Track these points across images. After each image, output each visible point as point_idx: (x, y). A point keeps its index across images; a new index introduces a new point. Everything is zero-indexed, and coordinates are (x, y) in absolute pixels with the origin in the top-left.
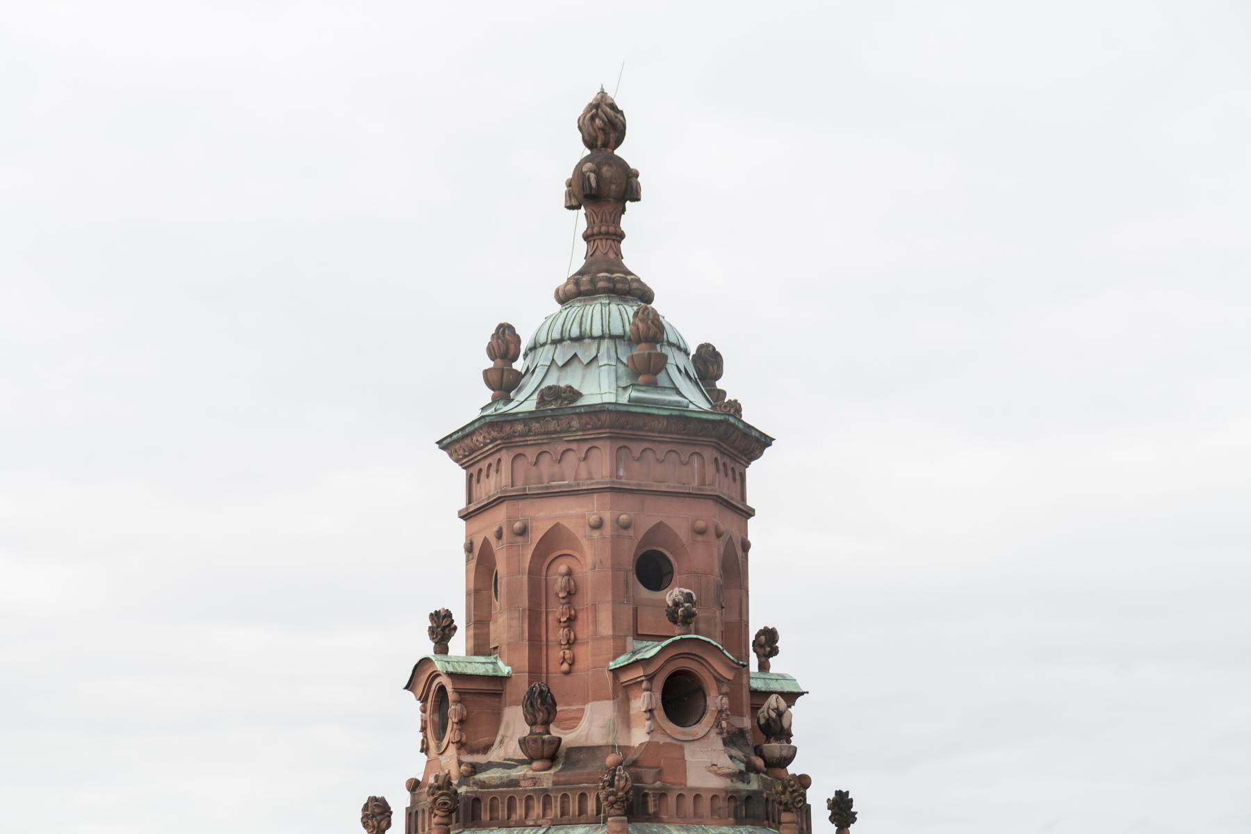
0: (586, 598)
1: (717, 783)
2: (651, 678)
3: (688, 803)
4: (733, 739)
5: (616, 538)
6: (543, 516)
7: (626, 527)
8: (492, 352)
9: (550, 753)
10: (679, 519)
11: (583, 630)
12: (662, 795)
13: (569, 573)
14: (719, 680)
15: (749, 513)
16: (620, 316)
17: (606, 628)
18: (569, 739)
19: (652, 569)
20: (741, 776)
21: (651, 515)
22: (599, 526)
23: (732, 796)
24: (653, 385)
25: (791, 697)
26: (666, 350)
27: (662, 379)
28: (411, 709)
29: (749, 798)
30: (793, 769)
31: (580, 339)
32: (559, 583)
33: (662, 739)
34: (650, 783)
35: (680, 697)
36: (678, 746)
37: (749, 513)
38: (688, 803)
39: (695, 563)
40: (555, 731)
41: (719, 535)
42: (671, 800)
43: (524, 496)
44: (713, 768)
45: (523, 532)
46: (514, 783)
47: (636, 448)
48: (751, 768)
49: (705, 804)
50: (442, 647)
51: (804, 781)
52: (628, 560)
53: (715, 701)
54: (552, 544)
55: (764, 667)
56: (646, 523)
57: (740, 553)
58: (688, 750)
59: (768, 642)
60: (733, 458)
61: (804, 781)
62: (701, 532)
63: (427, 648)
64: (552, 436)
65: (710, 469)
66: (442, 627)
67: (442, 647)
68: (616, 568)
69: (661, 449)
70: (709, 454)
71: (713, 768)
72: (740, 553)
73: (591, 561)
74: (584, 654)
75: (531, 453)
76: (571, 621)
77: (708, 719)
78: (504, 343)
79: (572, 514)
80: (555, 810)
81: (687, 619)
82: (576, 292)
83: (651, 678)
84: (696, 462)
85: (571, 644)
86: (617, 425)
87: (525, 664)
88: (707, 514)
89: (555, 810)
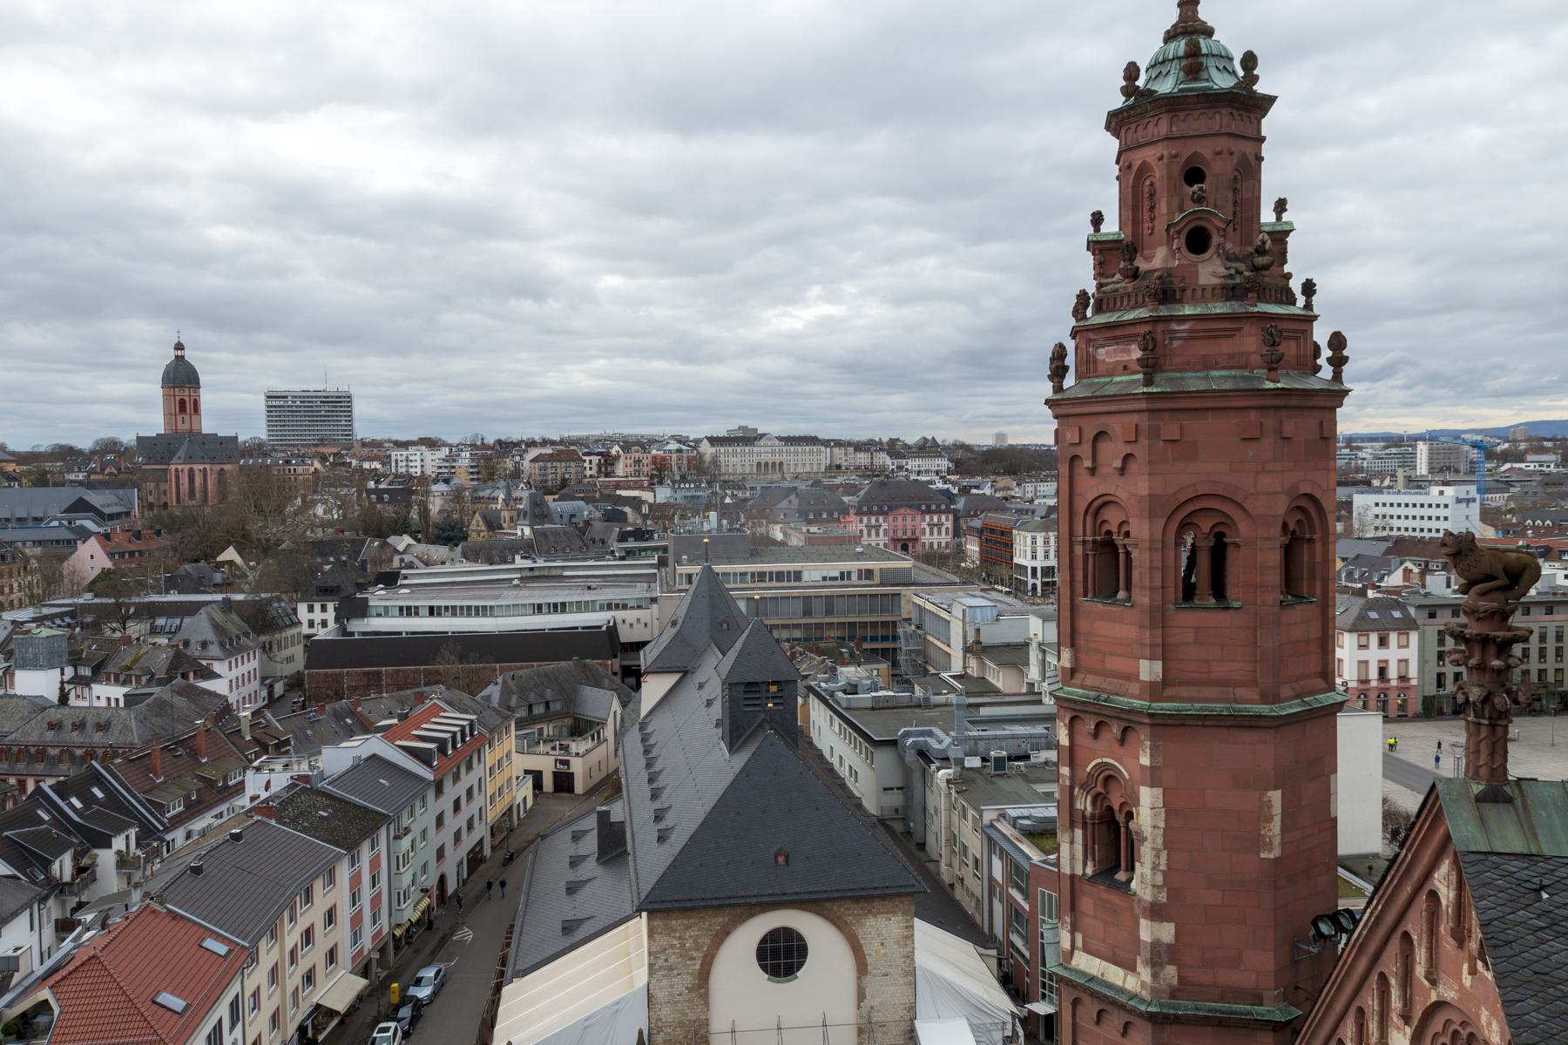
0: (1158, 195)
1: (1215, 281)
2: (1179, 232)
3: (1199, 292)
4: (1229, 258)
5: (1169, 163)
6: (1138, 158)
7: (1175, 156)
8: (1125, 78)
9: (1135, 275)
10: (1205, 149)
11: (1157, 211)
12: (1183, 290)
13: (1152, 184)
14: (1218, 229)
15: (1263, 139)
16: (1180, 46)
17: (1164, 210)
18: (1142, 265)
19: (1194, 175)
20: (1231, 276)
21: (1187, 149)
22: (1161, 159)
23: (1223, 287)
24: (1196, 80)
25: (1287, 233)
26: (1204, 60)
27: (1204, 75)
28: (1089, 259)
29: (1234, 287)
30: (1287, 269)
31: (1163, 62)
32: (1146, 189)
33: (1184, 262)
34: (1178, 284)
35: (1198, 241)
36: (1195, 265)
37: (1263, 139)
38: (1199, 292)
39: (1220, 170)
40: (1136, 263)
41: (1231, 154)
42: (1189, 292)
43: (1129, 149)
44: (1214, 274)
45: (1129, 167)
46: (1116, 290)
47: (1182, 115)
48: (1239, 272)
49: (1209, 291)
50: (1097, 229)
51: (1289, 276)
52: (1177, 170)
53: (1216, 239)
54: (1144, 171)
55: (1279, 218)
56: (1186, 154)
57: (1253, 161)
58: (1200, 266)
59: (1281, 206)
60: (1247, 111)
61: (1289, 276)
62: (1219, 153)
63: (1091, 230)
64: (1141, 116)
65: (1226, 120)
66: (1097, 219)
67: (1097, 229)
68: (1169, 178)
69: (1196, 114)
70: (1224, 111)
71: (1214, 274)
72: (1253, 161)
73: (1159, 173)
74: (1156, 222)
75: (1133, 126)
76: (1152, 208)
77: (1212, 250)
78: (1132, 72)
79: (1149, 155)
80: (1133, 302)
81: (1199, 200)
82: (1170, 37)
83: (1179, 232)
84: (1218, 117)
85: (1152, 220)
86: (1172, 104)
87: (1130, 232)
88: (1223, 143)
89: (1133, 302)
